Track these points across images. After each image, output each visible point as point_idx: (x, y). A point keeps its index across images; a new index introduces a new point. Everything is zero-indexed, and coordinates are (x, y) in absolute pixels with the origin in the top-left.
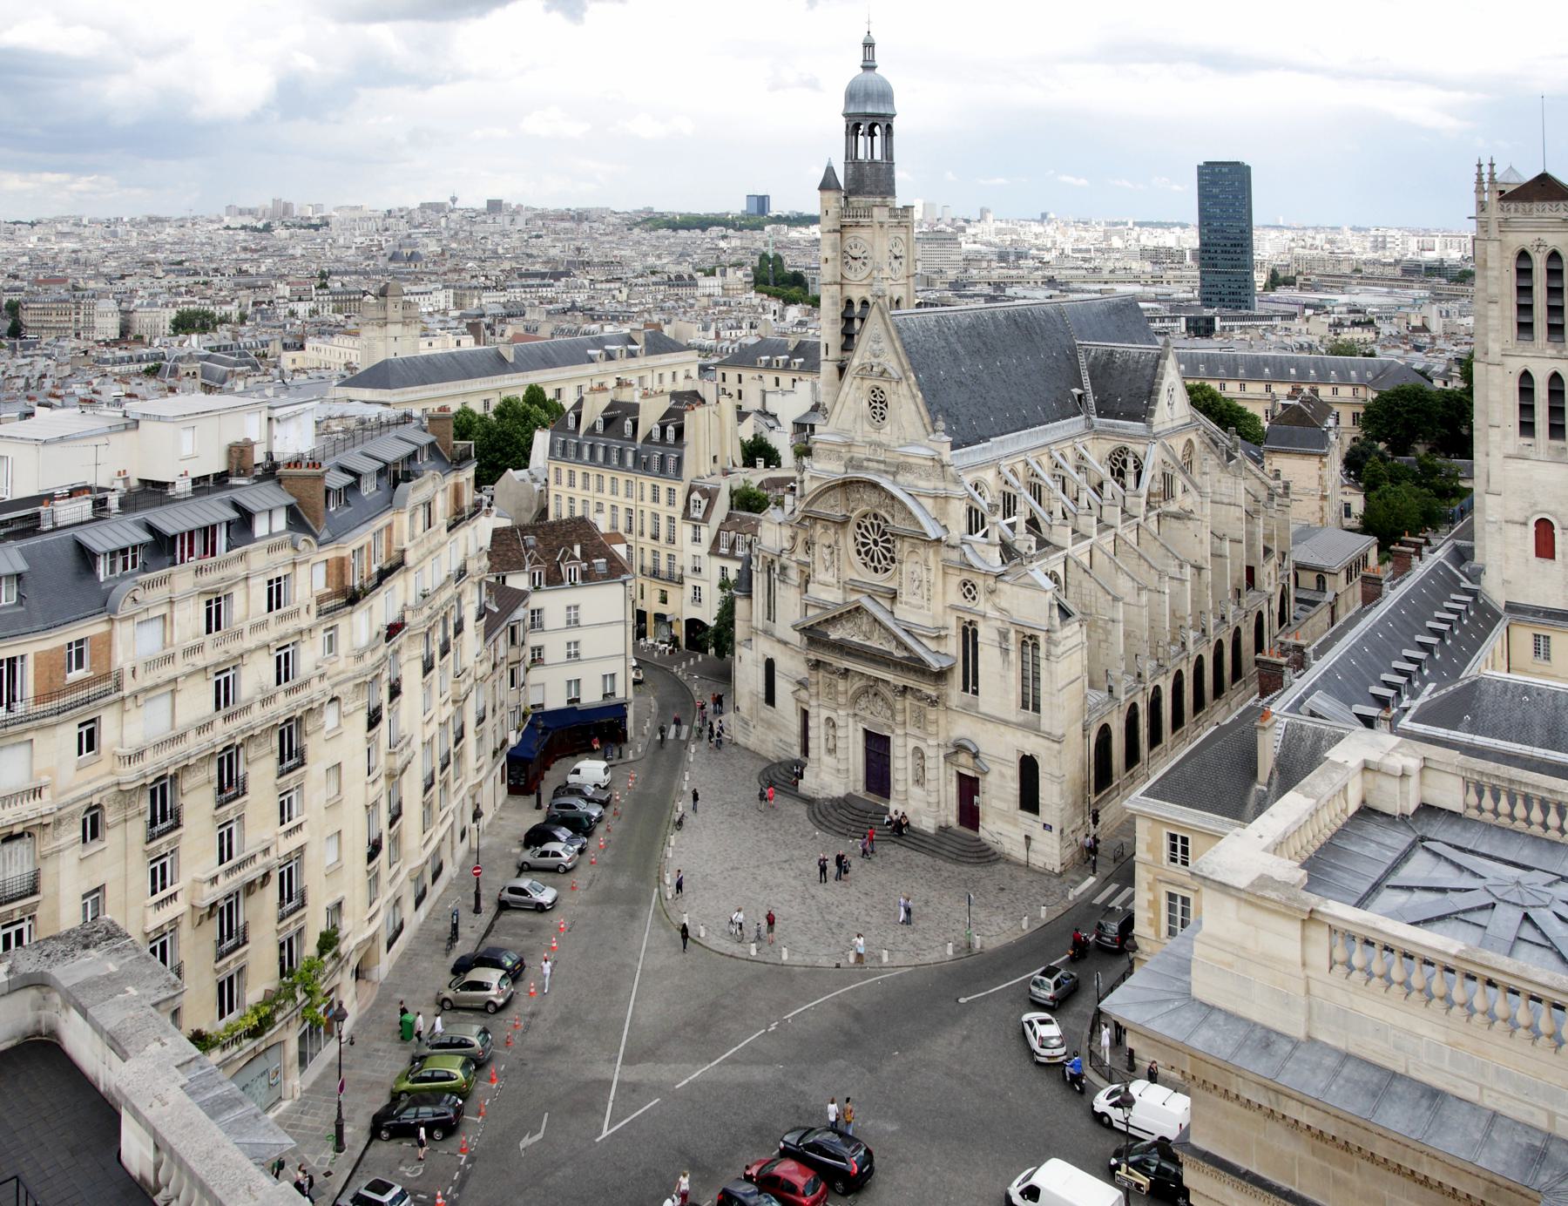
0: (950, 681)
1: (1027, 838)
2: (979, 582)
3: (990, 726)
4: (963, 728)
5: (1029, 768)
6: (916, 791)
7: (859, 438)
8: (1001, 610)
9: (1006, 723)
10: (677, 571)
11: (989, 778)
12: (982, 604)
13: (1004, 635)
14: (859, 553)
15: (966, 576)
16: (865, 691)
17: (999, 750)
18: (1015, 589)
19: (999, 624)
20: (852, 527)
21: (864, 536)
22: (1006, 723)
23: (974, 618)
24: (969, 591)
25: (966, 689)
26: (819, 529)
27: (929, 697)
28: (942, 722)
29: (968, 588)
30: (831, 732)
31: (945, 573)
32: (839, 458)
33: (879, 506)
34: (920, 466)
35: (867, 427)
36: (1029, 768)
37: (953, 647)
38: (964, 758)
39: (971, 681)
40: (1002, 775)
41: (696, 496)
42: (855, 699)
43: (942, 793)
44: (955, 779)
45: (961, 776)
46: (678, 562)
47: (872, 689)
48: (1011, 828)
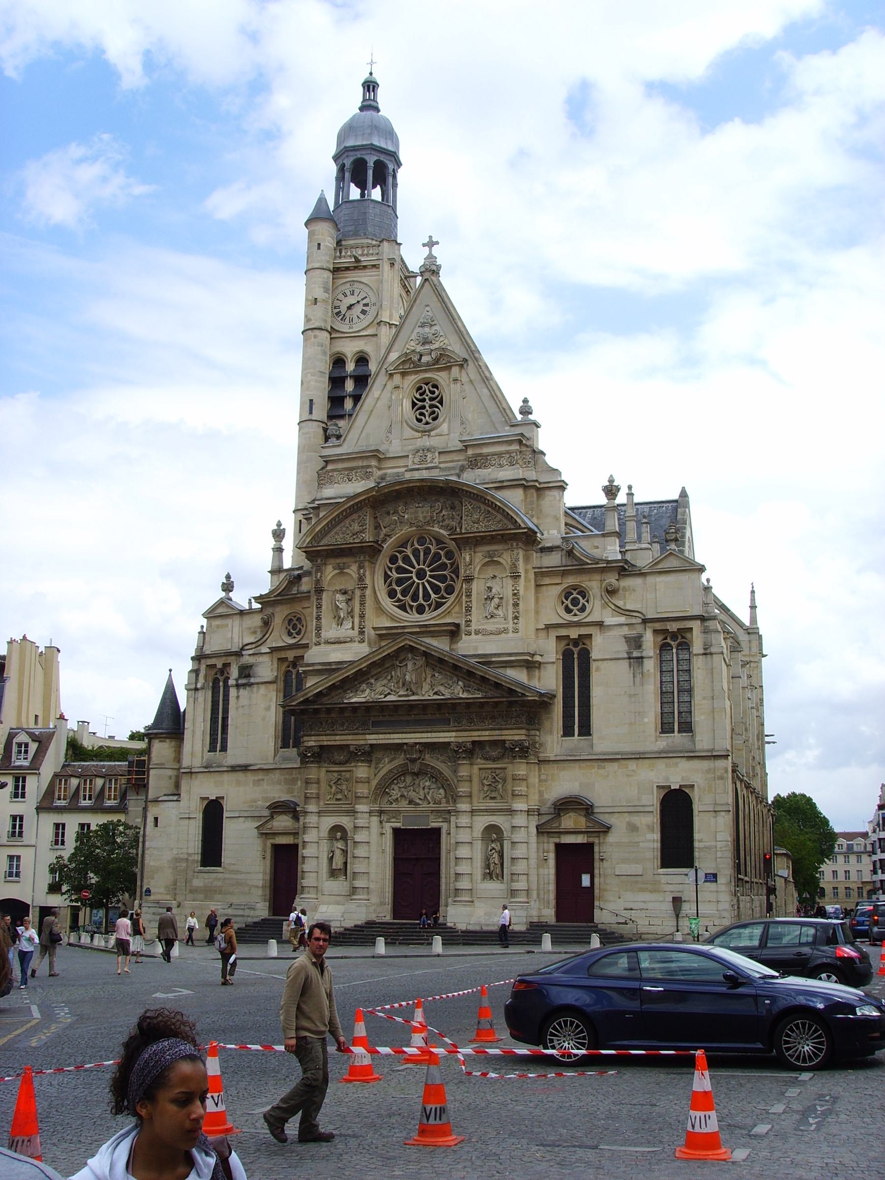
0: (547, 724)
1: (677, 902)
2: (594, 585)
3: (612, 767)
4: (565, 783)
5: (676, 809)
7: (395, 448)
8: (627, 613)
9: (639, 757)
11: (611, 838)
12: (597, 610)
13: (635, 642)
14: (392, 594)
15: (571, 581)
16: (400, 774)
17: (626, 797)
18: (650, 579)
19: (625, 631)
20: (383, 561)
21: (400, 570)
22: (639, 757)
23: (584, 631)
24: (575, 602)
25: (568, 731)
26: (330, 571)
27: (519, 743)
28: (534, 779)
29: (574, 598)
30: (340, 845)
31: (538, 586)
32: (367, 476)
33: (431, 521)
34: (500, 455)
35: (409, 433)
36: (676, 809)
37: (549, 680)
38: (569, 821)
39: (579, 722)
42: (382, 790)
43: (533, 878)
44: (552, 856)
45: (560, 848)
47: (414, 765)
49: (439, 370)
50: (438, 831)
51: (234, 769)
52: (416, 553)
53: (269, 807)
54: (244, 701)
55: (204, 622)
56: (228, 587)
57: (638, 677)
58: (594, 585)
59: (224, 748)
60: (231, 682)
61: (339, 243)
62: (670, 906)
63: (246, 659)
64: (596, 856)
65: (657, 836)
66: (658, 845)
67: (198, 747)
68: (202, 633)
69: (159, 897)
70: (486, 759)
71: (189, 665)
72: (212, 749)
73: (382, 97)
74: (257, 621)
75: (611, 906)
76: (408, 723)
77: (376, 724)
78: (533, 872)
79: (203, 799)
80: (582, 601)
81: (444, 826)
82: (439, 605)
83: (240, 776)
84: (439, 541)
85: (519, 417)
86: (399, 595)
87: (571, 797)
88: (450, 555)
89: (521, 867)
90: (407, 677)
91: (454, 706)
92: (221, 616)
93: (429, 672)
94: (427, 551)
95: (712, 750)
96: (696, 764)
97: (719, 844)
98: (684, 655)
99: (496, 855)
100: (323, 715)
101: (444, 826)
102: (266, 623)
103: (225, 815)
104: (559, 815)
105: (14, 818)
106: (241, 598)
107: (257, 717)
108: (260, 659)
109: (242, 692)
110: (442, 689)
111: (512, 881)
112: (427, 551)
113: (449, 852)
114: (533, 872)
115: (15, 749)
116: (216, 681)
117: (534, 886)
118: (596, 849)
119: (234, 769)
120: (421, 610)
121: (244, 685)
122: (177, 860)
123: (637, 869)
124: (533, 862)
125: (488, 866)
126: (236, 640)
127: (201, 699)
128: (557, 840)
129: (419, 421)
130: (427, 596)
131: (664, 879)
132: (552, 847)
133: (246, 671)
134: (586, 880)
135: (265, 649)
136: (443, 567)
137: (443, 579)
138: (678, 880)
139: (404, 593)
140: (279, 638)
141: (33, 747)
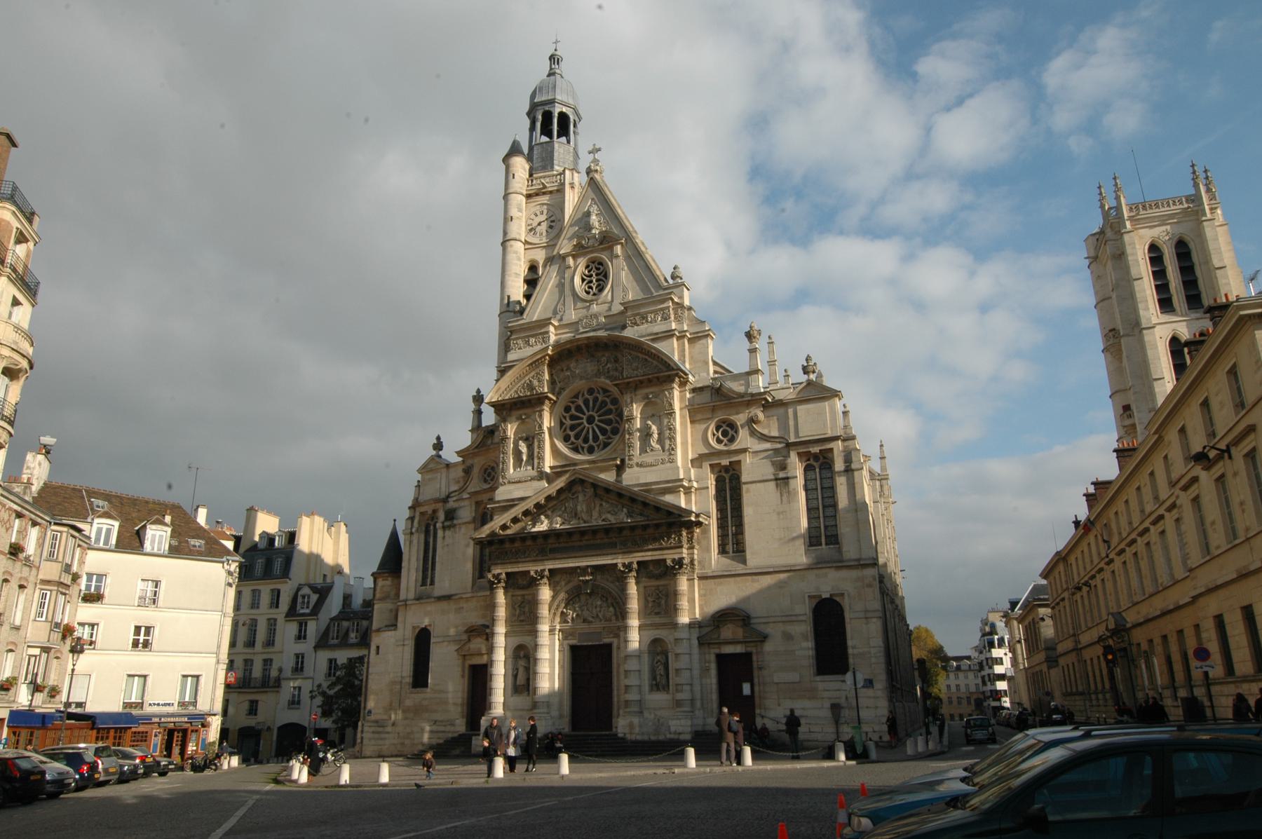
1: (836, 708)
2: (740, 419)
6: (660, 698)
10: (274, 673)
11: (768, 647)
12: (744, 439)
15: (721, 416)
21: (573, 418)
24: (725, 434)
30: (522, 663)
33: (598, 374)
38: (728, 632)
40: (788, 637)
41: (306, 591)
43: (697, 688)
45: (721, 658)
46: (275, 666)
48: (807, 703)
49: (603, 250)
50: (609, 646)
51: (441, 598)
52: (586, 402)
53: (466, 632)
54: (448, 541)
55: (419, 477)
56: (438, 446)
57: (785, 498)
58: (740, 419)
59: (432, 583)
60: (439, 525)
61: (531, 175)
62: (827, 713)
63: (451, 504)
64: (755, 665)
65: (810, 644)
66: (811, 653)
67: (412, 584)
68: (418, 486)
69: (378, 717)
70: (649, 578)
71: (407, 514)
72: (424, 584)
73: (564, 68)
74: (459, 473)
75: (772, 714)
76: (580, 548)
77: (553, 551)
78: (697, 682)
79: (414, 628)
80: (731, 432)
81: (615, 641)
82: (606, 445)
83: (444, 605)
84: (605, 391)
85: (671, 282)
86: (572, 439)
87: (727, 609)
88: (615, 401)
89: (684, 677)
90: (579, 508)
91: (621, 530)
92: (431, 470)
93: (598, 502)
94: (596, 399)
95: (859, 560)
96: (844, 573)
97: (873, 651)
98: (826, 474)
99: (661, 667)
100: (507, 545)
101: (615, 641)
102: (468, 471)
103: (432, 640)
104: (718, 627)
105: (297, 656)
106: (450, 455)
107: (456, 553)
108: (462, 504)
109: (448, 533)
110: (609, 516)
111: (677, 691)
112: (596, 399)
113: (619, 666)
114: (697, 682)
115: (300, 600)
116: (427, 526)
117: (698, 696)
118: (754, 658)
119: (441, 598)
120: (591, 451)
121: (449, 527)
122: (394, 683)
123: (794, 677)
124: (696, 672)
125: (654, 678)
126: (443, 489)
127: (415, 542)
128: (717, 651)
129: (588, 293)
130: (596, 438)
131: (821, 686)
132: (713, 658)
133: (451, 515)
134: (746, 689)
135: (465, 496)
136: (609, 412)
137: (609, 422)
138: (833, 687)
139: (577, 437)
140: (475, 485)
141: (314, 597)
